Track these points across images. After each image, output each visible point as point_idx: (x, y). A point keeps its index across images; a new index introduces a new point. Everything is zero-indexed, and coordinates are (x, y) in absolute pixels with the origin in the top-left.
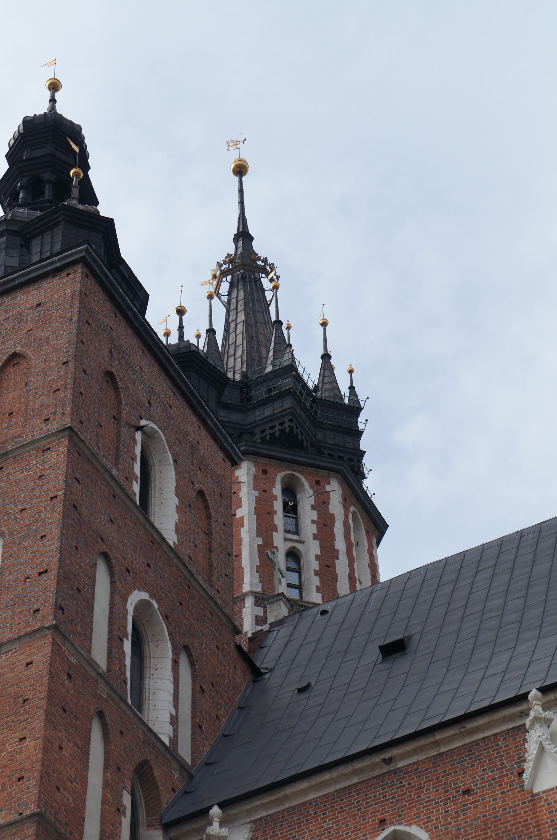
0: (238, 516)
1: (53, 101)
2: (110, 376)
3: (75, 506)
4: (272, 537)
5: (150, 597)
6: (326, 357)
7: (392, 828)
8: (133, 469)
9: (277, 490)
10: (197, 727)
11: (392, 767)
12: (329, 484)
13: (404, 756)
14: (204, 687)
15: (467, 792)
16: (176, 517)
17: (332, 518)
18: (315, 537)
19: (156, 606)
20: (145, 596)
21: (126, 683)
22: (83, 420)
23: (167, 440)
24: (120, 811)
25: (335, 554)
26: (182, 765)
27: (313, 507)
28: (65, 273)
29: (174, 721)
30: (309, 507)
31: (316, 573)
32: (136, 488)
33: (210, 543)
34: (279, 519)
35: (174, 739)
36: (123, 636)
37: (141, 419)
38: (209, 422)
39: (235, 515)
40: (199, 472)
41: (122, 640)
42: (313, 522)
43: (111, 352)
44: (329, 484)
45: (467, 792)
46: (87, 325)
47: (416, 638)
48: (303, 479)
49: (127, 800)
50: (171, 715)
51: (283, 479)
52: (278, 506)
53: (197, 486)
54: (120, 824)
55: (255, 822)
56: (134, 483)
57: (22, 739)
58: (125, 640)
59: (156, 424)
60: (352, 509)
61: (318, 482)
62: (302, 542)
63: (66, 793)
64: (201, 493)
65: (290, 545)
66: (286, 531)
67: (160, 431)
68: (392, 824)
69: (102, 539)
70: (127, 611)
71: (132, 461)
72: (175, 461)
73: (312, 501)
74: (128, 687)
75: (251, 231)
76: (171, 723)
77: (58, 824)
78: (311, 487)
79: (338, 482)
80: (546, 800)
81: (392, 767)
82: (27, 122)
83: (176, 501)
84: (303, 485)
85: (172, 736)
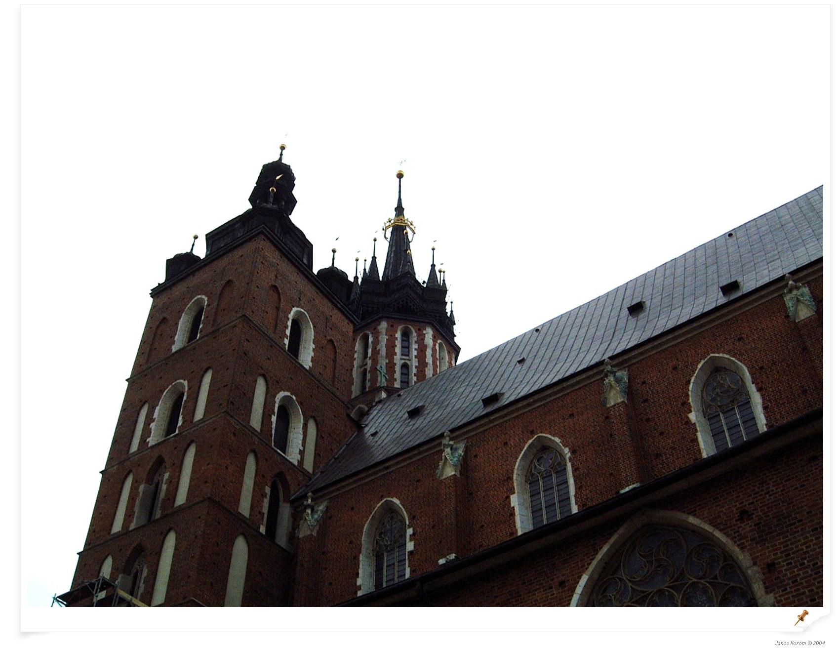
0: (378, 349)
1: (281, 155)
2: (275, 288)
3: (245, 353)
4: (393, 358)
5: (291, 394)
6: (433, 266)
7: (385, 499)
8: (285, 332)
9: (398, 335)
10: (317, 454)
11: (388, 471)
12: (425, 330)
13: (393, 465)
14: (323, 436)
15: (418, 481)
16: (312, 354)
17: (426, 347)
18: (416, 357)
19: (294, 398)
20: (288, 394)
21: (271, 436)
22: (254, 311)
23: (310, 317)
24: (263, 495)
25: (426, 365)
26: (305, 473)
27: (416, 342)
28: (254, 239)
29: (302, 453)
30: (414, 342)
31: (415, 375)
32: (287, 341)
33: (335, 365)
34: (398, 350)
35: (301, 462)
36: (272, 414)
37: (294, 307)
38: (339, 305)
39: (376, 348)
40: (330, 330)
41: (271, 416)
42: (415, 349)
43: (276, 276)
44: (425, 330)
45: (418, 481)
46: (261, 264)
47: (426, 407)
48: (410, 327)
49: (268, 490)
50: (300, 450)
51: (402, 329)
52: (398, 343)
53: (328, 338)
54: (263, 502)
55: (330, 498)
56: (285, 339)
57: (208, 464)
58: (273, 416)
59: (303, 309)
60: (439, 341)
61: (419, 330)
62: (409, 360)
63: (228, 488)
64: (331, 341)
65: (403, 361)
66: (402, 355)
67: (305, 313)
68: (386, 498)
69: (261, 367)
70: (275, 402)
71: (284, 328)
72: (314, 327)
73: (415, 339)
74: (273, 438)
75: (403, 206)
76: (300, 454)
77: (223, 502)
78: (416, 332)
79: (431, 328)
80: (445, 483)
81: (388, 471)
82: (264, 166)
83: (313, 346)
84: (412, 332)
85: (299, 459)
